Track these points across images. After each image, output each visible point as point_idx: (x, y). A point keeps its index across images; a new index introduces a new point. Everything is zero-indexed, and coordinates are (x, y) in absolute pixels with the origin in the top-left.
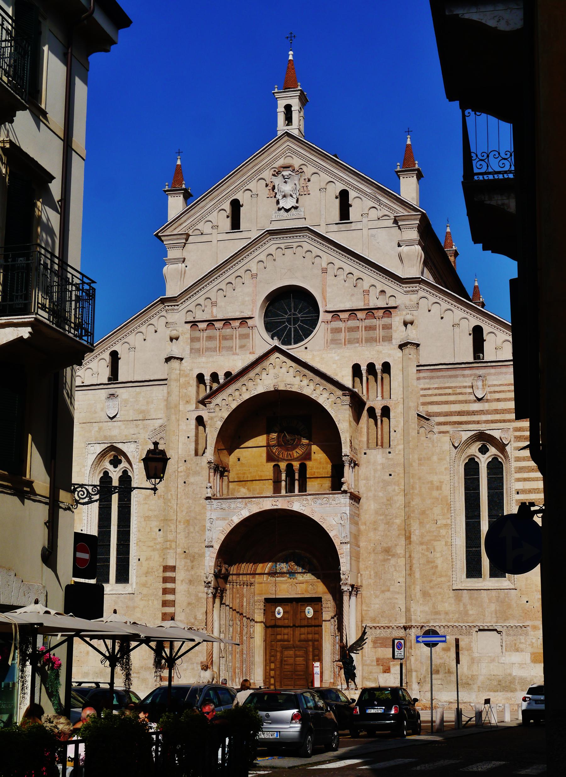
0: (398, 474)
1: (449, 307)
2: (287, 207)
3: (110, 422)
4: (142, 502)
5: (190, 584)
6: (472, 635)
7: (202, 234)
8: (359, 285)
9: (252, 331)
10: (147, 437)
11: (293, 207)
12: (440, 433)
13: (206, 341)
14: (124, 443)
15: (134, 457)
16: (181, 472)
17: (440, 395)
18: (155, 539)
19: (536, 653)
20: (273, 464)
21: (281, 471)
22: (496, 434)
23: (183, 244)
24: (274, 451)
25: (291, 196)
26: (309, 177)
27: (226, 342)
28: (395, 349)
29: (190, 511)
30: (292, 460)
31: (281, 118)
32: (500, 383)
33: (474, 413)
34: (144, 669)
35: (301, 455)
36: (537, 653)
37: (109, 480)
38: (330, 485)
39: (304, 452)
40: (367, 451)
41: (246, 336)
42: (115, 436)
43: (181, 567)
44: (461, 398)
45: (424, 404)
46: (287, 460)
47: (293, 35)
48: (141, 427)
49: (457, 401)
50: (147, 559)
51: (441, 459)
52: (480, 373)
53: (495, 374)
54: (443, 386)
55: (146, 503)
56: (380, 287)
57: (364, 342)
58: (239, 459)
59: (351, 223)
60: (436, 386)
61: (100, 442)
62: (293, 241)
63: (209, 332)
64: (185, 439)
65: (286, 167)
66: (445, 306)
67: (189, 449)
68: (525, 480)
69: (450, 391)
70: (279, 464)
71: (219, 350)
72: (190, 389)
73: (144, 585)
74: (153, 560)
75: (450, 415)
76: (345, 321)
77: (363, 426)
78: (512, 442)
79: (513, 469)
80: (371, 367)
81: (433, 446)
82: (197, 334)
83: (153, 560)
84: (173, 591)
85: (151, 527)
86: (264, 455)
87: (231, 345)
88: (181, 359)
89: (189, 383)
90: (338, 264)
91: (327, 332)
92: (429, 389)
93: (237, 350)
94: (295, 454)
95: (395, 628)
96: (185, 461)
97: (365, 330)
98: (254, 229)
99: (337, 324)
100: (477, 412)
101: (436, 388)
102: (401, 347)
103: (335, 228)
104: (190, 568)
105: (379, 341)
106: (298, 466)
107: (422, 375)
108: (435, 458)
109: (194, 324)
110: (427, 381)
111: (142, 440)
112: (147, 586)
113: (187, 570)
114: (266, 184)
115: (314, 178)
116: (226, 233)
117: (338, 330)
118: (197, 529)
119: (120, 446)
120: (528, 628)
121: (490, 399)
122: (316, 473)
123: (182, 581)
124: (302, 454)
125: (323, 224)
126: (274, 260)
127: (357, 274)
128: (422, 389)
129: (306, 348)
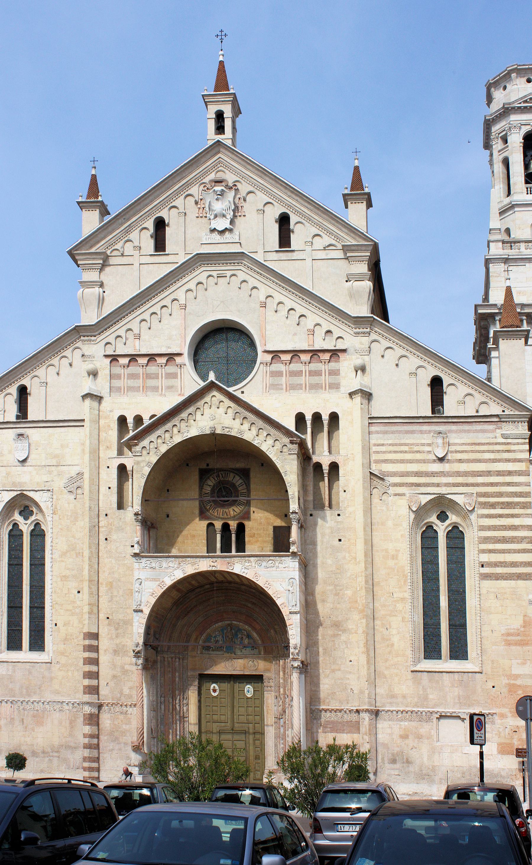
0: (349, 540)
1: (404, 353)
2: (220, 229)
3: (19, 466)
4: (58, 559)
5: (115, 655)
6: (432, 722)
7: (122, 255)
8: (302, 323)
9: (181, 370)
10: (62, 485)
11: (226, 229)
12: (396, 495)
13: (127, 379)
14: (36, 491)
15: (47, 507)
16: (102, 527)
17: (395, 452)
18: (74, 602)
19: (504, 743)
20: (206, 522)
21: (216, 531)
22: (459, 499)
23: (100, 265)
24: (208, 508)
25: (224, 216)
26: (244, 195)
27: (151, 381)
28: (343, 398)
29: (113, 573)
30: (228, 518)
31: (211, 125)
32: (462, 441)
33: (433, 474)
34: (64, 748)
35: (239, 514)
36: (506, 743)
37: (18, 533)
38: (272, 548)
39: (242, 511)
40: (313, 513)
41: (174, 376)
42: (26, 483)
43: (103, 635)
44: (418, 456)
45: (377, 462)
46: (222, 519)
47: (223, 33)
48: (55, 473)
49: (414, 460)
50: (65, 625)
51: (397, 525)
52: (441, 429)
53: (456, 432)
54: (398, 442)
55: (63, 561)
56: (326, 326)
57: (307, 388)
58: (168, 516)
59: (293, 251)
60: (390, 442)
61: (8, 489)
62: (227, 269)
63: (133, 369)
64: (106, 489)
65: (218, 182)
66: (400, 352)
67: (111, 501)
68: (490, 551)
69: (406, 448)
70: (214, 522)
71: (143, 390)
72: (110, 432)
73: (62, 654)
74: (73, 626)
75: (406, 476)
76: (286, 364)
77: (308, 483)
78: (476, 509)
79: (477, 539)
80: (317, 417)
81: (388, 510)
82: (117, 370)
83: (73, 626)
84: (96, 662)
85: (68, 588)
86: (197, 512)
87: (157, 385)
88: (99, 399)
89: (109, 426)
90: (279, 298)
91: (266, 376)
92: (383, 445)
93: (163, 391)
94: (232, 513)
95: (348, 712)
96: (106, 515)
97: (310, 375)
98: (182, 253)
99: (277, 367)
100: (436, 473)
101: (390, 445)
102: (351, 395)
103: (275, 256)
104: (114, 637)
105: (326, 389)
106: (236, 525)
107: (373, 428)
108: (390, 523)
109: (114, 358)
110: (381, 435)
111: (57, 489)
112: (65, 655)
113: (111, 639)
114: (196, 200)
115: (250, 198)
116: (151, 255)
117: (279, 374)
118: (121, 592)
119: (31, 494)
120: (495, 715)
121: (451, 460)
122: (256, 535)
123: (105, 651)
124: (240, 513)
125: (261, 251)
126: (206, 290)
127: (300, 310)
128: (375, 445)
129: (243, 392)
